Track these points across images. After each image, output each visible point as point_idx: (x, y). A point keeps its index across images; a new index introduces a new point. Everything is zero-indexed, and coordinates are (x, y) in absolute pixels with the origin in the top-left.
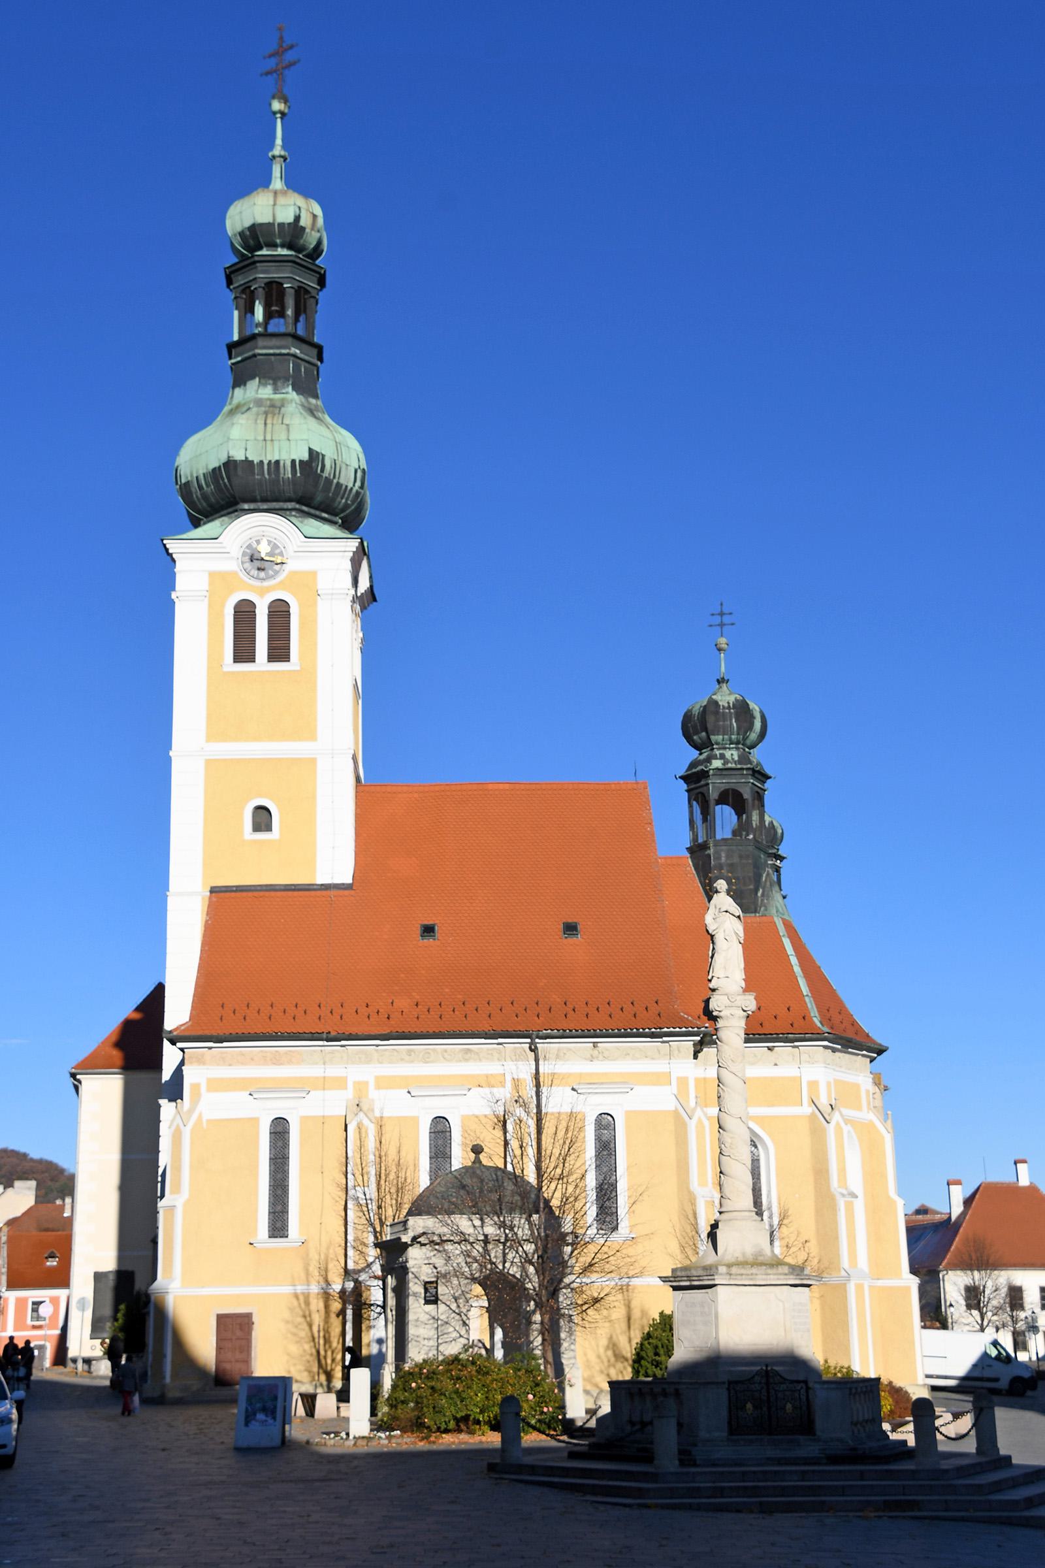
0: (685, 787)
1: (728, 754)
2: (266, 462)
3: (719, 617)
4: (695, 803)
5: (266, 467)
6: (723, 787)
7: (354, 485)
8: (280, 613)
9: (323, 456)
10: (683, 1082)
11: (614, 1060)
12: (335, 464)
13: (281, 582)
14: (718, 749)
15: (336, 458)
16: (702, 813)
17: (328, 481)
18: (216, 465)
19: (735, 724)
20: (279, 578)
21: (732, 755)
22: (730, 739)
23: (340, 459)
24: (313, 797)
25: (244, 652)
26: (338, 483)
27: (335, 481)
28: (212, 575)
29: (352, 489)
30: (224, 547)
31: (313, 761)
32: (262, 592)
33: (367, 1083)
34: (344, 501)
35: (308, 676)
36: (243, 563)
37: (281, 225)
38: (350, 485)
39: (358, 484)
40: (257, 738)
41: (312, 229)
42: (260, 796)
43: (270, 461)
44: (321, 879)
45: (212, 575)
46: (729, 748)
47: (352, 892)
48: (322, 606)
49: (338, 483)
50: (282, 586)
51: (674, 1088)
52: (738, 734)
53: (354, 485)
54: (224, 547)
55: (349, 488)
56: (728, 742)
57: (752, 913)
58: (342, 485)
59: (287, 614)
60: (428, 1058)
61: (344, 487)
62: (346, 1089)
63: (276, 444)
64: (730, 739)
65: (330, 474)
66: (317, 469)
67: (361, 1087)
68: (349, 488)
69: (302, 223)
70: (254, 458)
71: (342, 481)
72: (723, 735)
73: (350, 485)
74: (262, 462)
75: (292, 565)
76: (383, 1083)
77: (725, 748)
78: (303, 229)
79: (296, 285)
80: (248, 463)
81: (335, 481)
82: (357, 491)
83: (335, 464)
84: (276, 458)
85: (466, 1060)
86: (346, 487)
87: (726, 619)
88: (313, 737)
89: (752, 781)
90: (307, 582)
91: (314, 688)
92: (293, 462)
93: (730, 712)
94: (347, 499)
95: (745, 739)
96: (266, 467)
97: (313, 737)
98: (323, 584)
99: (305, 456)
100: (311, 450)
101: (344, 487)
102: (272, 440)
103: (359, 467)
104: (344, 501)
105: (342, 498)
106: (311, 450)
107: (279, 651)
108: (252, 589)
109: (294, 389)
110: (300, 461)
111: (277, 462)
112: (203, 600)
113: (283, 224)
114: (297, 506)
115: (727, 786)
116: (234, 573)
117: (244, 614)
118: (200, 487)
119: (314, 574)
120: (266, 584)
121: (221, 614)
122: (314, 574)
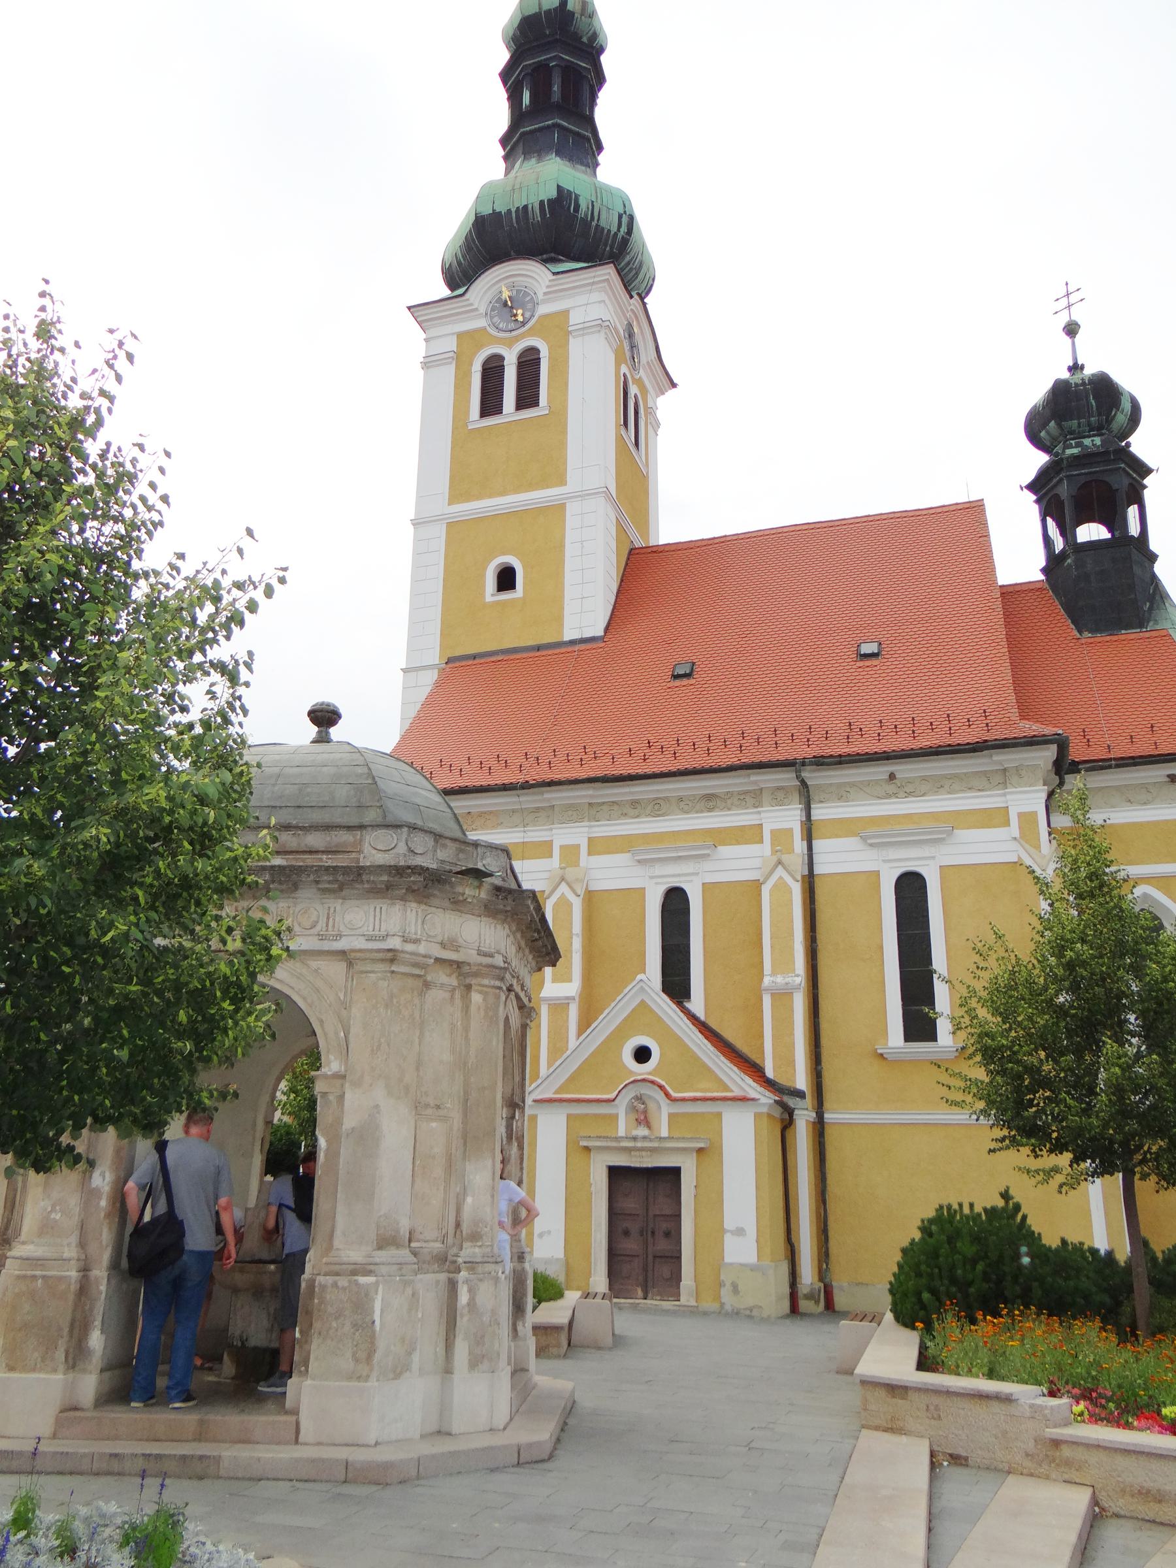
0: (1034, 498)
1: (1087, 442)
2: (513, 210)
3: (1065, 299)
4: (1049, 520)
5: (514, 215)
6: (1083, 480)
7: (619, 230)
8: (529, 364)
9: (577, 197)
10: (1027, 819)
11: (923, 795)
12: (593, 206)
13: (530, 329)
14: (1073, 439)
15: (594, 200)
16: (1061, 535)
17: (586, 223)
18: (468, 229)
19: (1093, 402)
20: (527, 326)
21: (1093, 441)
22: (1089, 424)
23: (599, 201)
24: (561, 547)
25: (491, 404)
26: (597, 226)
27: (594, 224)
28: (461, 336)
29: (616, 234)
30: (471, 304)
31: (562, 507)
32: (510, 343)
33: (578, 846)
34: (608, 249)
35: (559, 416)
36: (492, 318)
37: (548, 12)
38: (614, 229)
39: (624, 229)
40: (503, 493)
41: (582, 15)
42: (504, 554)
43: (518, 208)
44: (567, 638)
45: (461, 336)
46: (1089, 437)
47: (602, 645)
48: (575, 345)
49: (597, 226)
50: (531, 333)
51: (1014, 829)
52: (1100, 414)
53: (619, 230)
54: (471, 304)
55: (612, 233)
56: (1087, 428)
57: (1136, 628)
58: (603, 229)
59: (537, 361)
60: (659, 810)
61: (606, 231)
62: (551, 856)
63: (525, 189)
64: (1089, 424)
65: (586, 215)
66: (570, 207)
67: (570, 854)
68: (612, 233)
69: (570, 7)
70: (501, 208)
71: (603, 223)
72: (1079, 419)
73: (614, 229)
74: (509, 211)
75: (542, 310)
76: (596, 846)
77: (1084, 437)
78: (572, 14)
79: (563, 64)
80: (496, 215)
81: (594, 224)
82: (623, 237)
83: (593, 206)
84: (524, 203)
85: (710, 810)
86: (609, 231)
87: (1073, 298)
88: (562, 482)
89: (1123, 465)
90: (558, 326)
91: (564, 431)
92: (542, 203)
93: (1085, 389)
94: (612, 247)
95: (1110, 420)
96: (514, 215)
97: (562, 482)
98: (575, 318)
99: (553, 194)
100: (560, 189)
101: (606, 231)
102: (521, 188)
103: (625, 212)
104: (608, 249)
105: (606, 246)
106: (560, 189)
107: (527, 397)
108: (500, 341)
109: (556, 155)
110: (549, 200)
111: (526, 207)
112: (451, 363)
113: (550, 10)
114: (553, 255)
115: (1089, 478)
116: (484, 329)
117: (492, 372)
118: (459, 263)
119: (566, 313)
120: (514, 333)
121: (468, 374)
122: (566, 313)
